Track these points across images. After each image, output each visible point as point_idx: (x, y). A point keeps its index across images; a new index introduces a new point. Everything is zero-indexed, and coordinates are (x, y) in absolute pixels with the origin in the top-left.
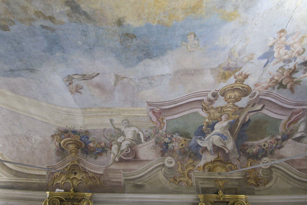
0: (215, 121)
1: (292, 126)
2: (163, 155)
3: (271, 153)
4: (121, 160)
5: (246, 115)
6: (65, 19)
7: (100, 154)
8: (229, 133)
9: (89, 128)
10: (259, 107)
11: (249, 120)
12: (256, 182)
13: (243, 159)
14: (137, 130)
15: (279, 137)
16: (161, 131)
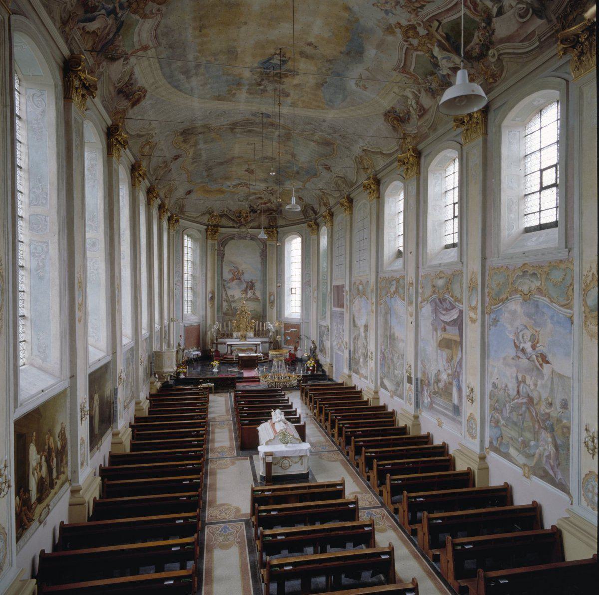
0: (430, 52)
1: (479, 9)
2: (434, 98)
3: (491, 43)
4: (421, 117)
5: (438, 33)
6: (332, 66)
7: (409, 119)
8: (447, 53)
9: (392, 105)
10: (436, 24)
11: (446, 34)
12: (494, 79)
13: (475, 64)
14: (410, 90)
15: (483, 25)
16: (420, 81)
